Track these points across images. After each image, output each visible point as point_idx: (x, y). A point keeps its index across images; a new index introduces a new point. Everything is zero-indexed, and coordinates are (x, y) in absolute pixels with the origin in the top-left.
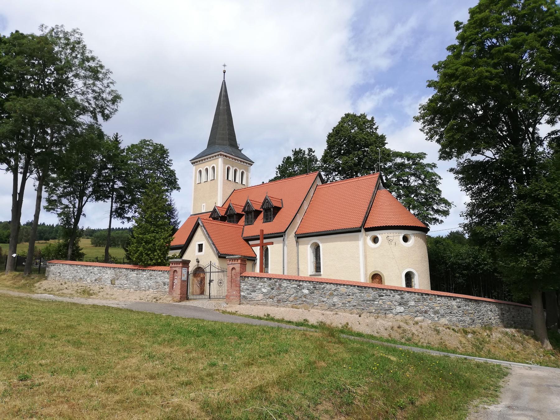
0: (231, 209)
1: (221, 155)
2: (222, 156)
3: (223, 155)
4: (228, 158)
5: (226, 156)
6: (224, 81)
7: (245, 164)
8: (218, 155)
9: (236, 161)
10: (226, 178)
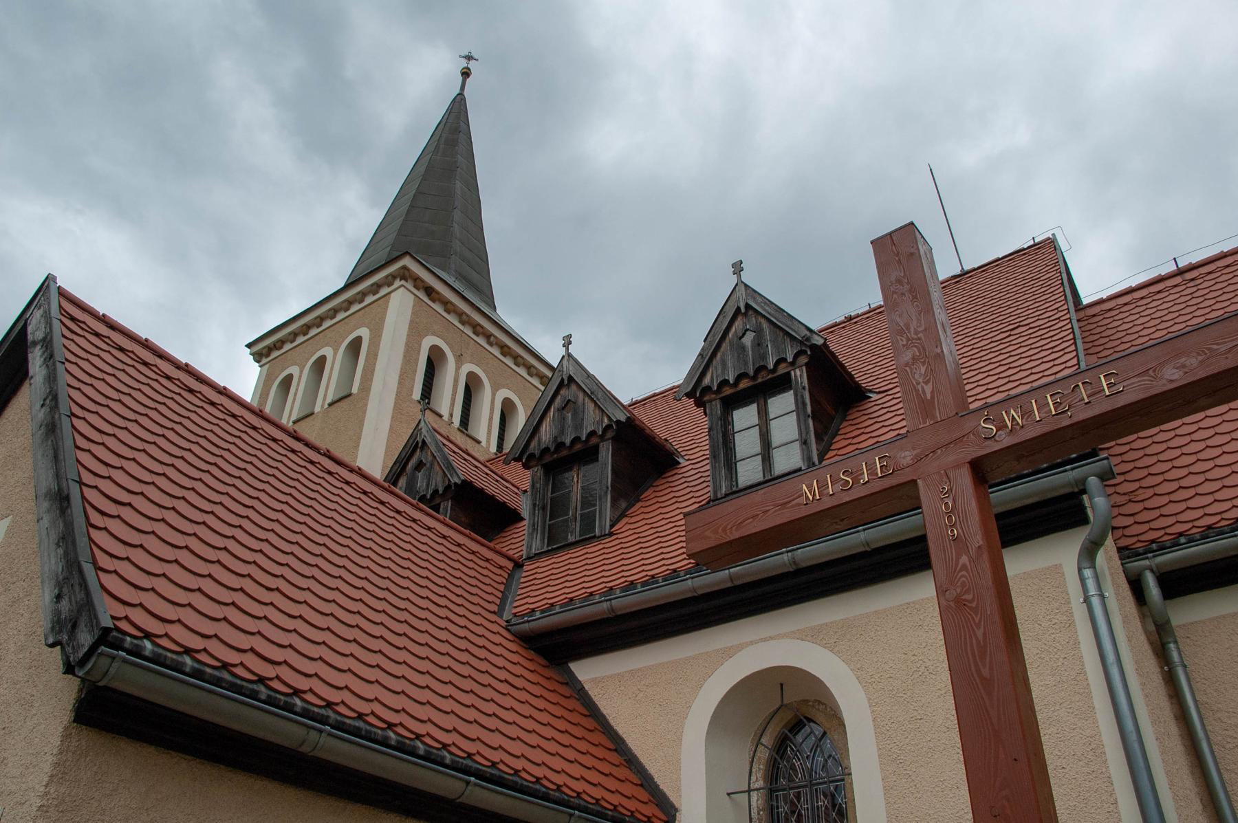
0: (420, 465)
1: (405, 274)
2: (409, 285)
3: (417, 282)
4: (438, 307)
5: (429, 291)
6: (461, 94)
7: (522, 372)
8: (389, 281)
9: (481, 341)
10: (417, 394)
